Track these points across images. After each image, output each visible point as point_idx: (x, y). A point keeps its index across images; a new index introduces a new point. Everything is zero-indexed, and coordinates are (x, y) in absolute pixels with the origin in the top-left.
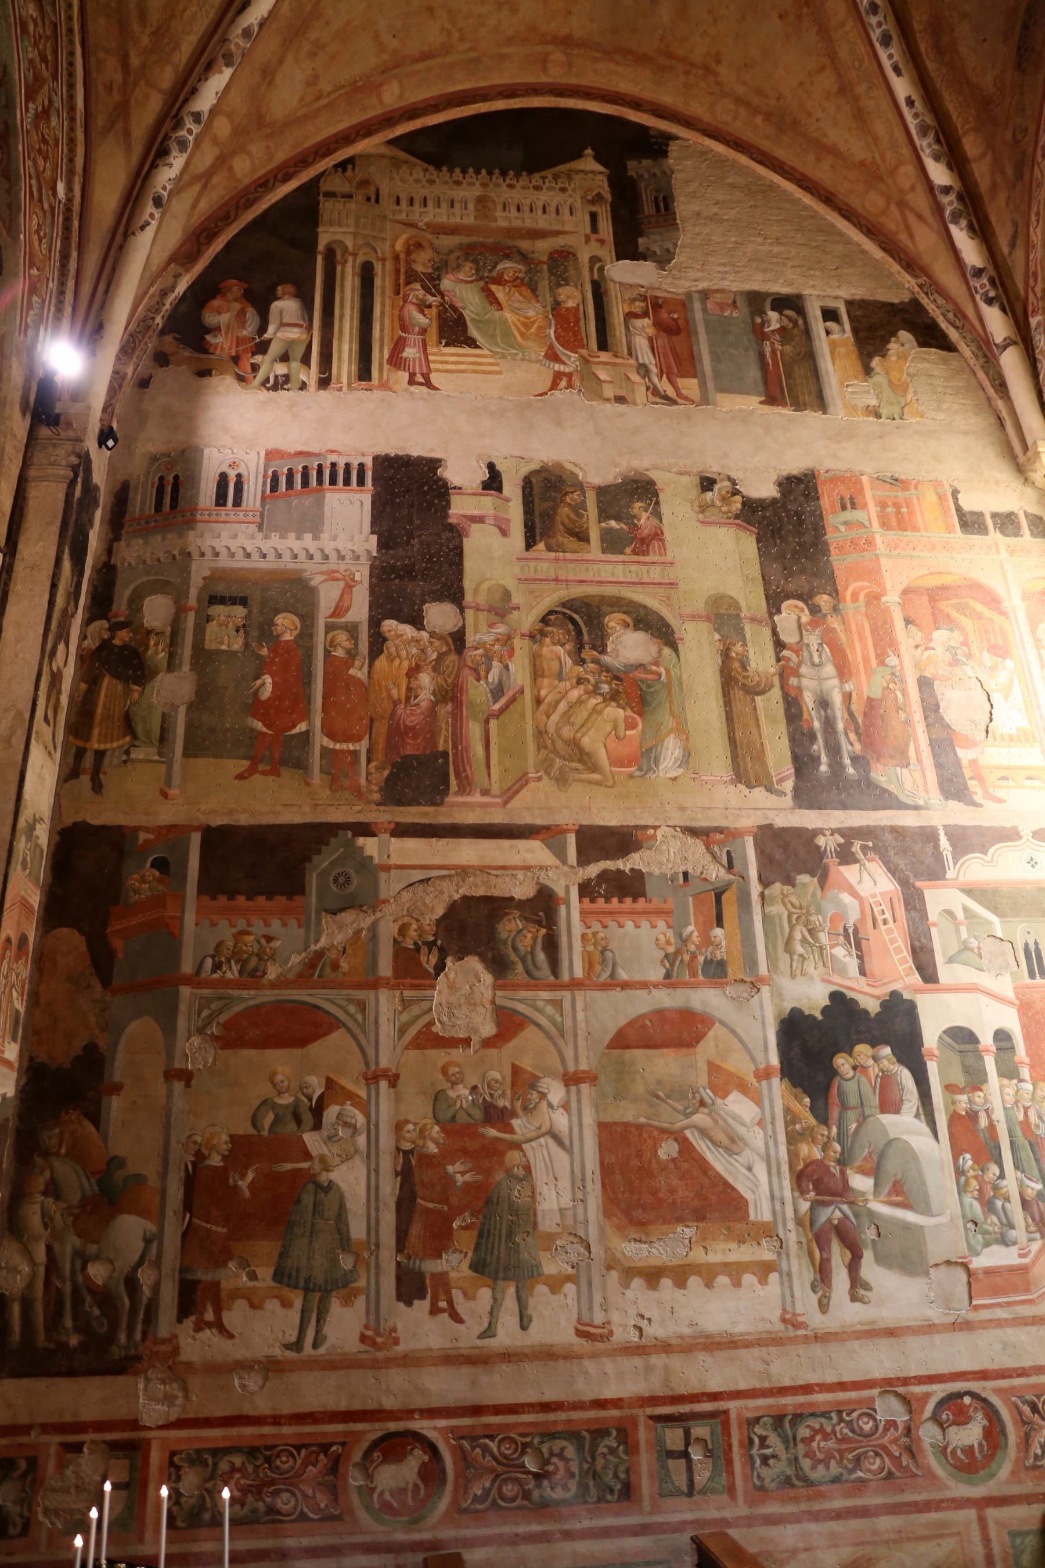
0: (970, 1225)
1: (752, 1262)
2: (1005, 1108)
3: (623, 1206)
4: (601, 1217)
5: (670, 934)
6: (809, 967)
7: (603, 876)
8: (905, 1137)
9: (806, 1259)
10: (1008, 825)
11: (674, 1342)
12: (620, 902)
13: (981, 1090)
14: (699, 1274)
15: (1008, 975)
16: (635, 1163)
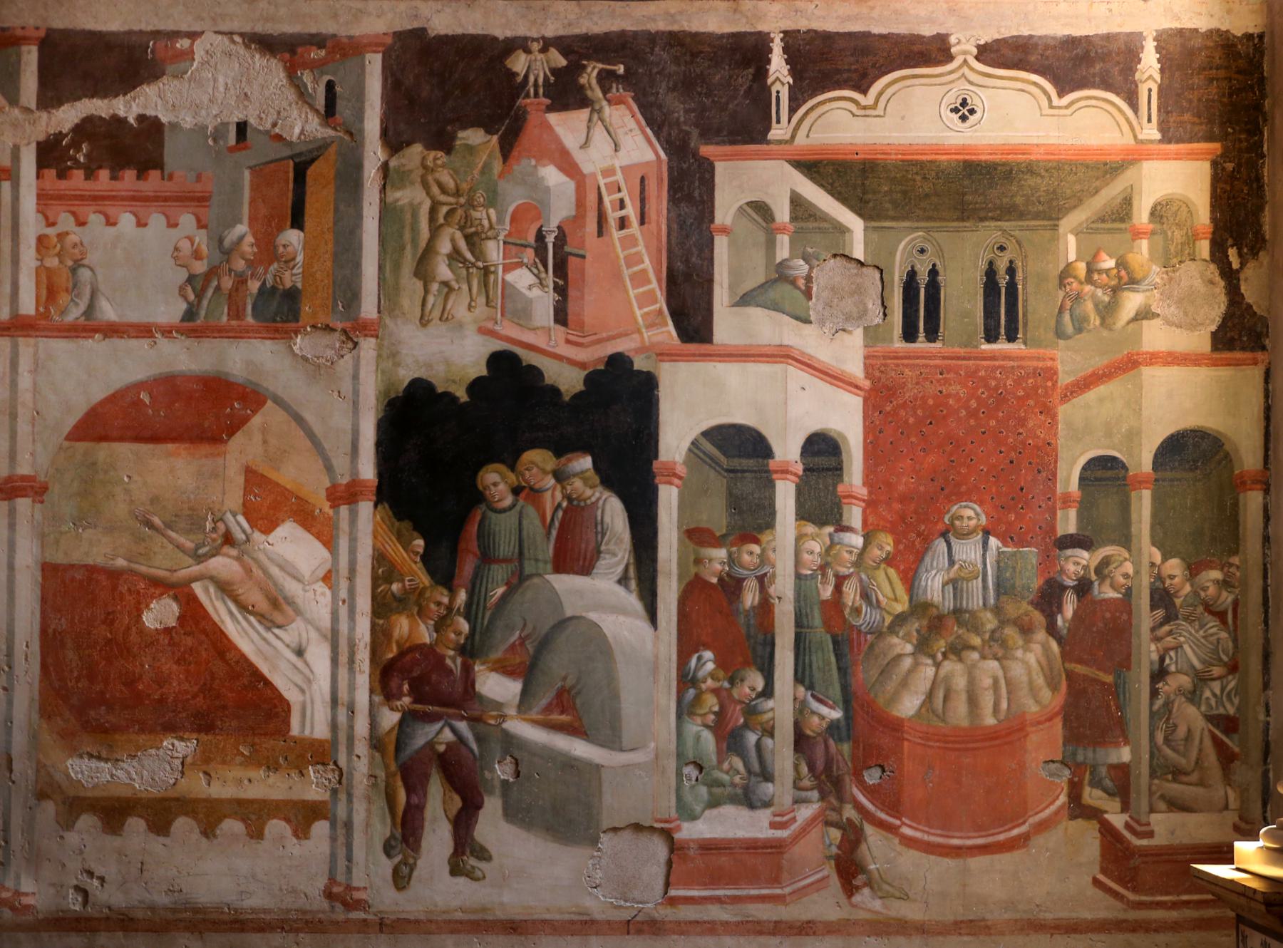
0: (690, 771)
1: (287, 803)
2: (798, 576)
3: (74, 701)
4: (35, 716)
5: (201, 238)
6: (458, 306)
7: (85, 128)
8: (593, 616)
9: (380, 803)
11: (139, 915)
12: (114, 178)
13: (756, 541)
14: (192, 813)
15: (858, 334)
16: (103, 632)
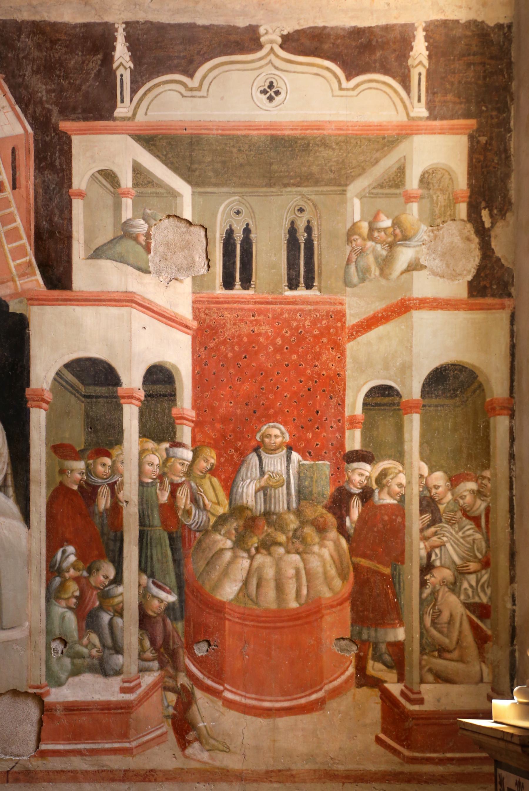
0: (57, 645)
2: (142, 484)
10: (242, 23)
13: (108, 455)
15: (188, 282)
